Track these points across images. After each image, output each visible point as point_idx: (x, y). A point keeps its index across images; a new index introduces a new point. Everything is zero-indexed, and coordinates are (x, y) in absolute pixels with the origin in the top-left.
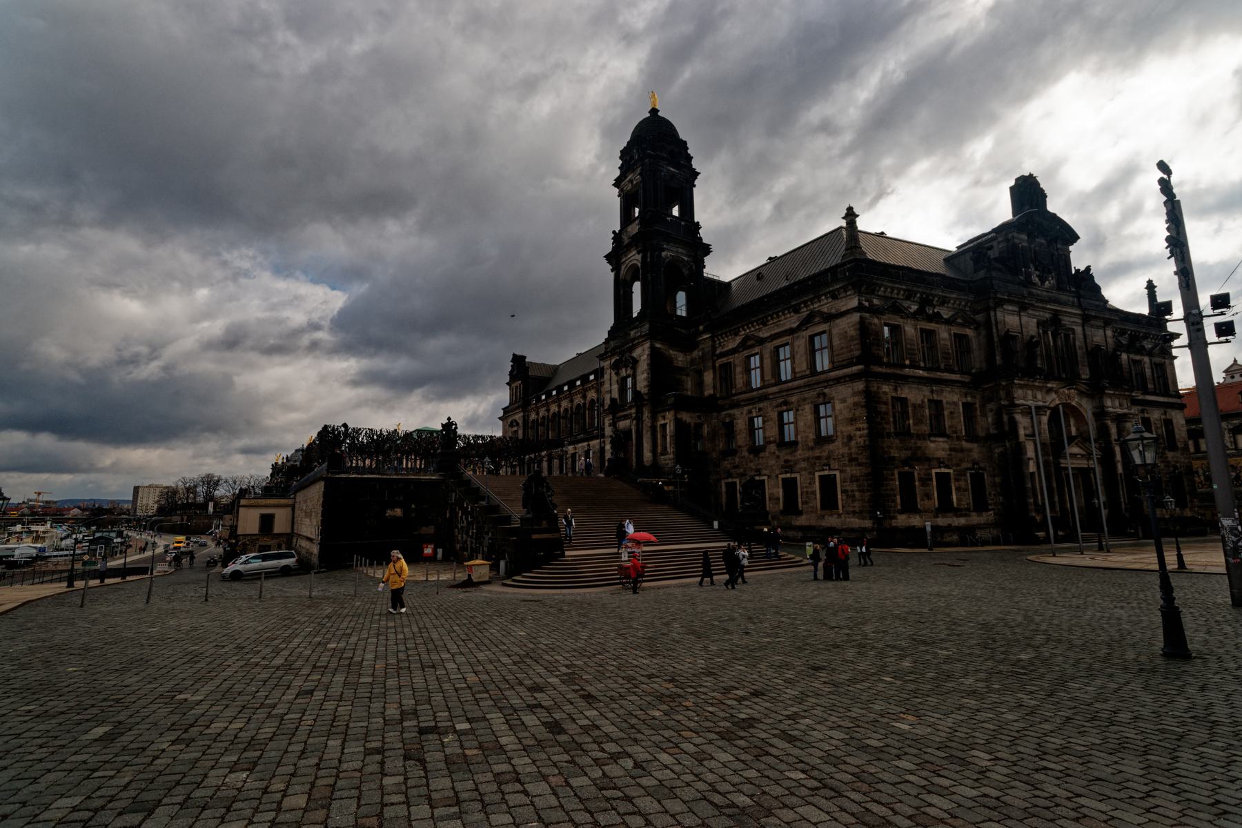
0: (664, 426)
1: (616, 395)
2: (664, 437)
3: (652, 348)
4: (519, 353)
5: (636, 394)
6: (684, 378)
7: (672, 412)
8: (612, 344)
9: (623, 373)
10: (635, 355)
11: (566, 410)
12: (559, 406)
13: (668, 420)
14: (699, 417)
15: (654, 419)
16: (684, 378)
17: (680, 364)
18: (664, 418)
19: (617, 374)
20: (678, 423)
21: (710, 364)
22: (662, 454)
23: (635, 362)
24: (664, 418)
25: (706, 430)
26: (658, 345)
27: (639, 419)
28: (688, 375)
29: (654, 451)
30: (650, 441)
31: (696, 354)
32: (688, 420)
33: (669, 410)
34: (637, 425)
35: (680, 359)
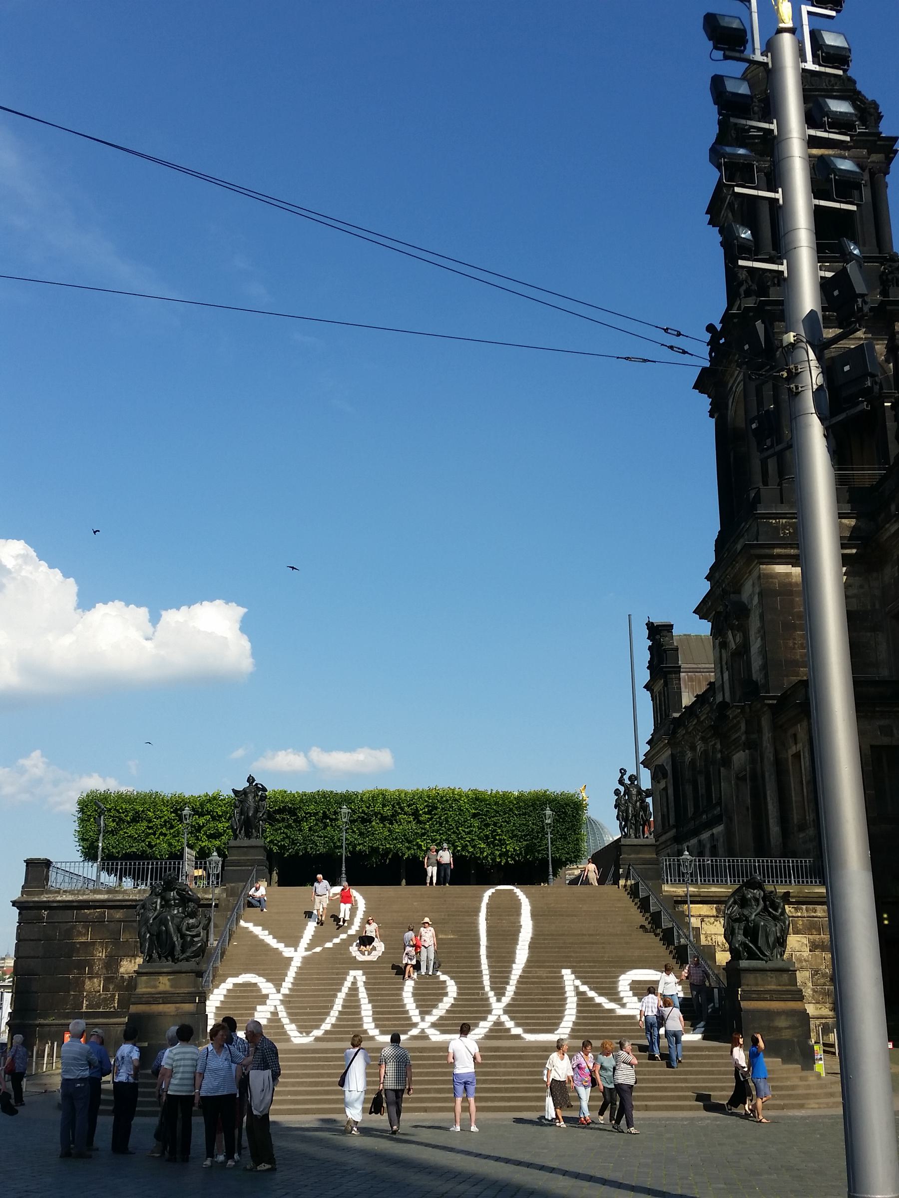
0: (797, 756)
4: (657, 620)
9: (733, 640)
27: (752, 745)
29: (784, 820)
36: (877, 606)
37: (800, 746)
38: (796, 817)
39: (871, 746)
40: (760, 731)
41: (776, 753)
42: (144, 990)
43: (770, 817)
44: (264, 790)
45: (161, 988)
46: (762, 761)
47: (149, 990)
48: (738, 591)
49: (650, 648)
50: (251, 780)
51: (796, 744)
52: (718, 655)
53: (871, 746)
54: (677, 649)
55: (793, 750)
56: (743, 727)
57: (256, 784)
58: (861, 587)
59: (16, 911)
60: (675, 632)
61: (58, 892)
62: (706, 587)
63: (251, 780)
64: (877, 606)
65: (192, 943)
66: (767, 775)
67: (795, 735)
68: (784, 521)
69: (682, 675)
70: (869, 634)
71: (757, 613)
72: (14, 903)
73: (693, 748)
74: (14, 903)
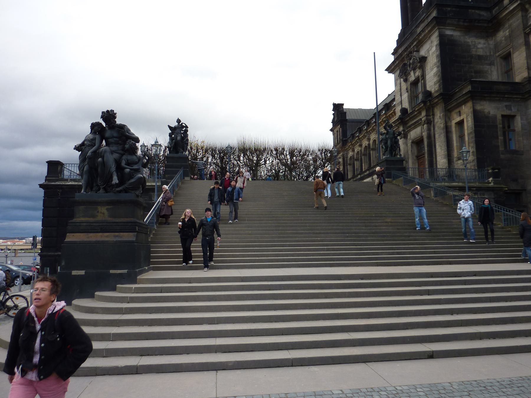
0: (460, 124)
1: (406, 105)
2: (461, 137)
3: (442, 37)
4: (337, 102)
5: (428, 94)
6: (486, 68)
7: (470, 104)
8: (400, 51)
9: (412, 77)
10: (423, 53)
11: (375, 141)
12: (369, 139)
13: (465, 114)
14: (508, 107)
15: (447, 118)
16: (486, 68)
17: (481, 52)
18: (460, 114)
19: (406, 80)
20: (477, 117)
21: (521, 40)
22: (459, 159)
23: (423, 59)
24: (460, 114)
25: (518, 123)
26: (448, 32)
27: (429, 122)
28: (491, 64)
30: (444, 148)
31: (502, 35)
32: (492, 112)
33: (464, 102)
34: (429, 129)
35: (479, 45)
36: (492, 53)
37: (463, 116)
38: (455, 154)
39: (503, 116)
40: (433, 115)
41: (446, 123)
42: (82, 219)
43: (438, 156)
44: (187, 127)
45: (100, 218)
46: (434, 129)
47: (87, 219)
48: (418, 51)
49: (333, 114)
50: (179, 121)
51: (460, 116)
52: (399, 88)
53: (503, 116)
54: (345, 113)
55: (458, 119)
56: (424, 113)
57: (182, 123)
58: (484, 44)
59: (42, 192)
60: (345, 107)
61: (67, 180)
62: (392, 59)
63: (179, 121)
64: (492, 53)
65: (131, 176)
66: (437, 136)
67: (460, 112)
68: (449, 9)
69: (348, 123)
70: (488, 67)
71: (435, 55)
72: (41, 186)
73: (353, 151)
74: (41, 186)
